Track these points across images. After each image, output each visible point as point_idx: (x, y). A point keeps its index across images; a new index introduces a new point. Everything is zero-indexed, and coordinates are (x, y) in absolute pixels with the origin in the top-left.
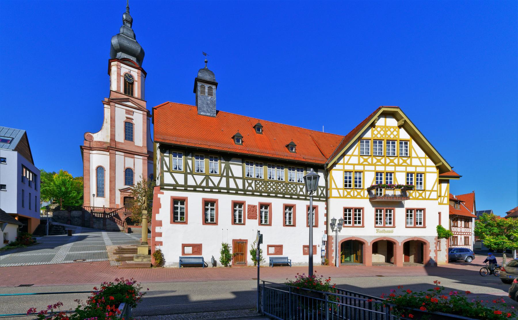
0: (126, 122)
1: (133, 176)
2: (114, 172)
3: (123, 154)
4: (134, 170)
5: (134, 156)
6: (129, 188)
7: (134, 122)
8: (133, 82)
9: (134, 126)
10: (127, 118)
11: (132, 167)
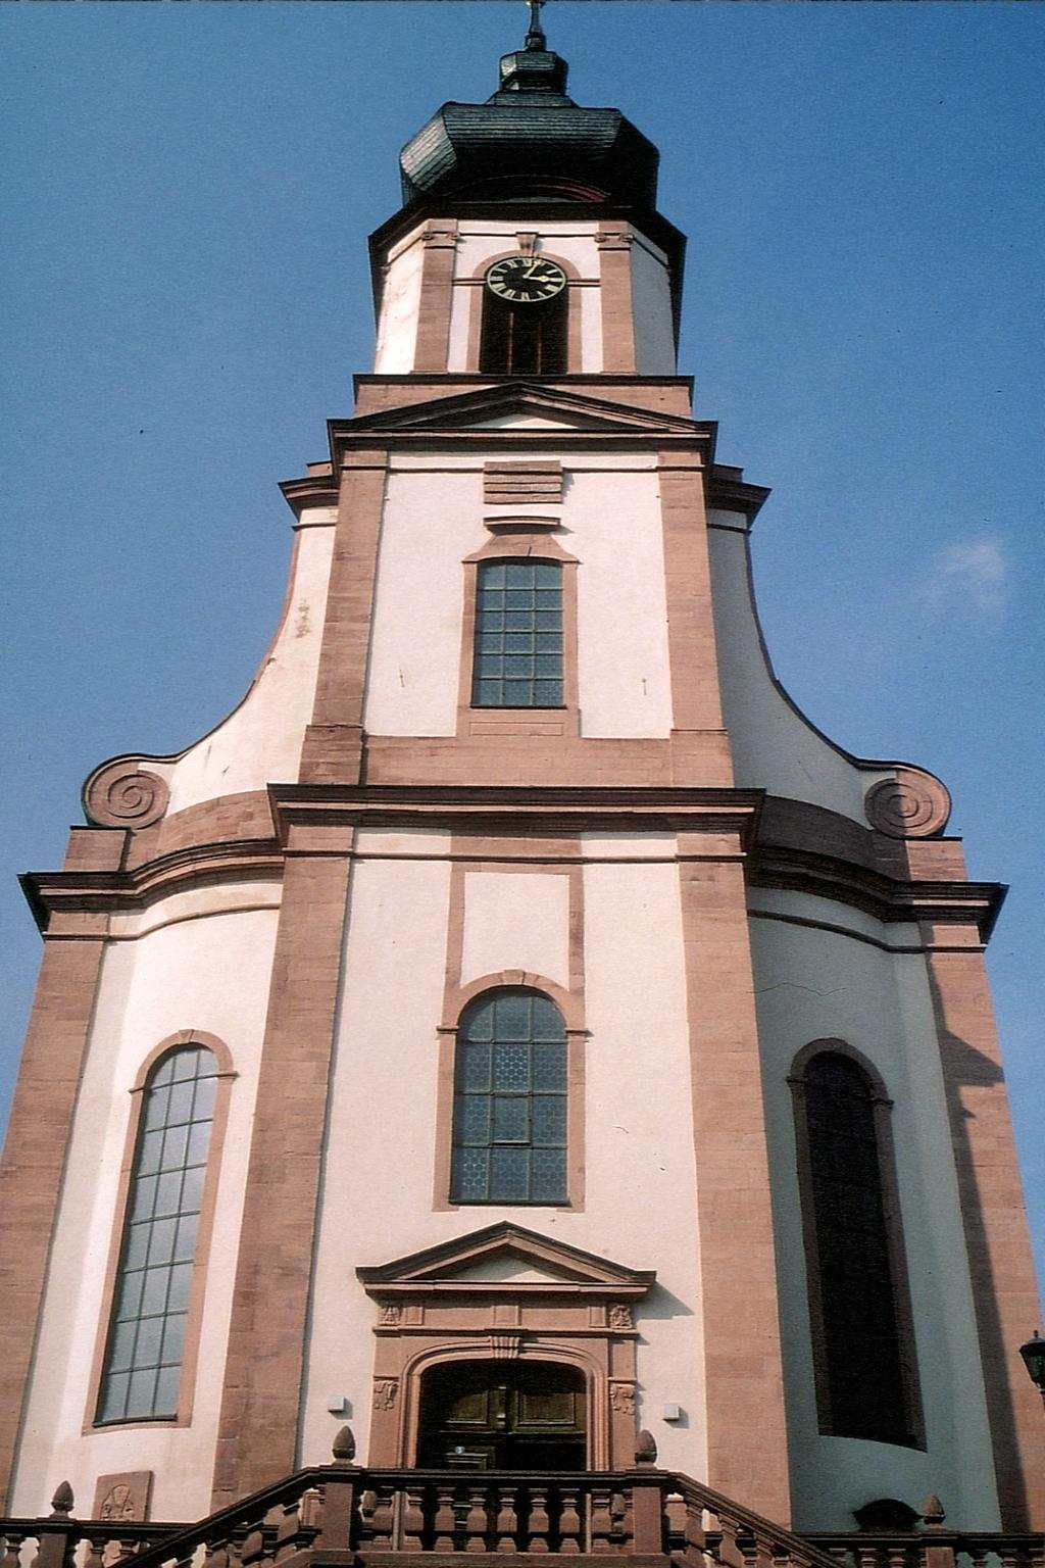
0: (485, 565)
1: (561, 1081)
2: (310, 1057)
3: (440, 842)
4: (579, 992)
5: (578, 848)
6: (503, 1228)
7: (566, 545)
8: (564, 294)
9: (574, 579)
10: (499, 527)
11: (550, 967)
